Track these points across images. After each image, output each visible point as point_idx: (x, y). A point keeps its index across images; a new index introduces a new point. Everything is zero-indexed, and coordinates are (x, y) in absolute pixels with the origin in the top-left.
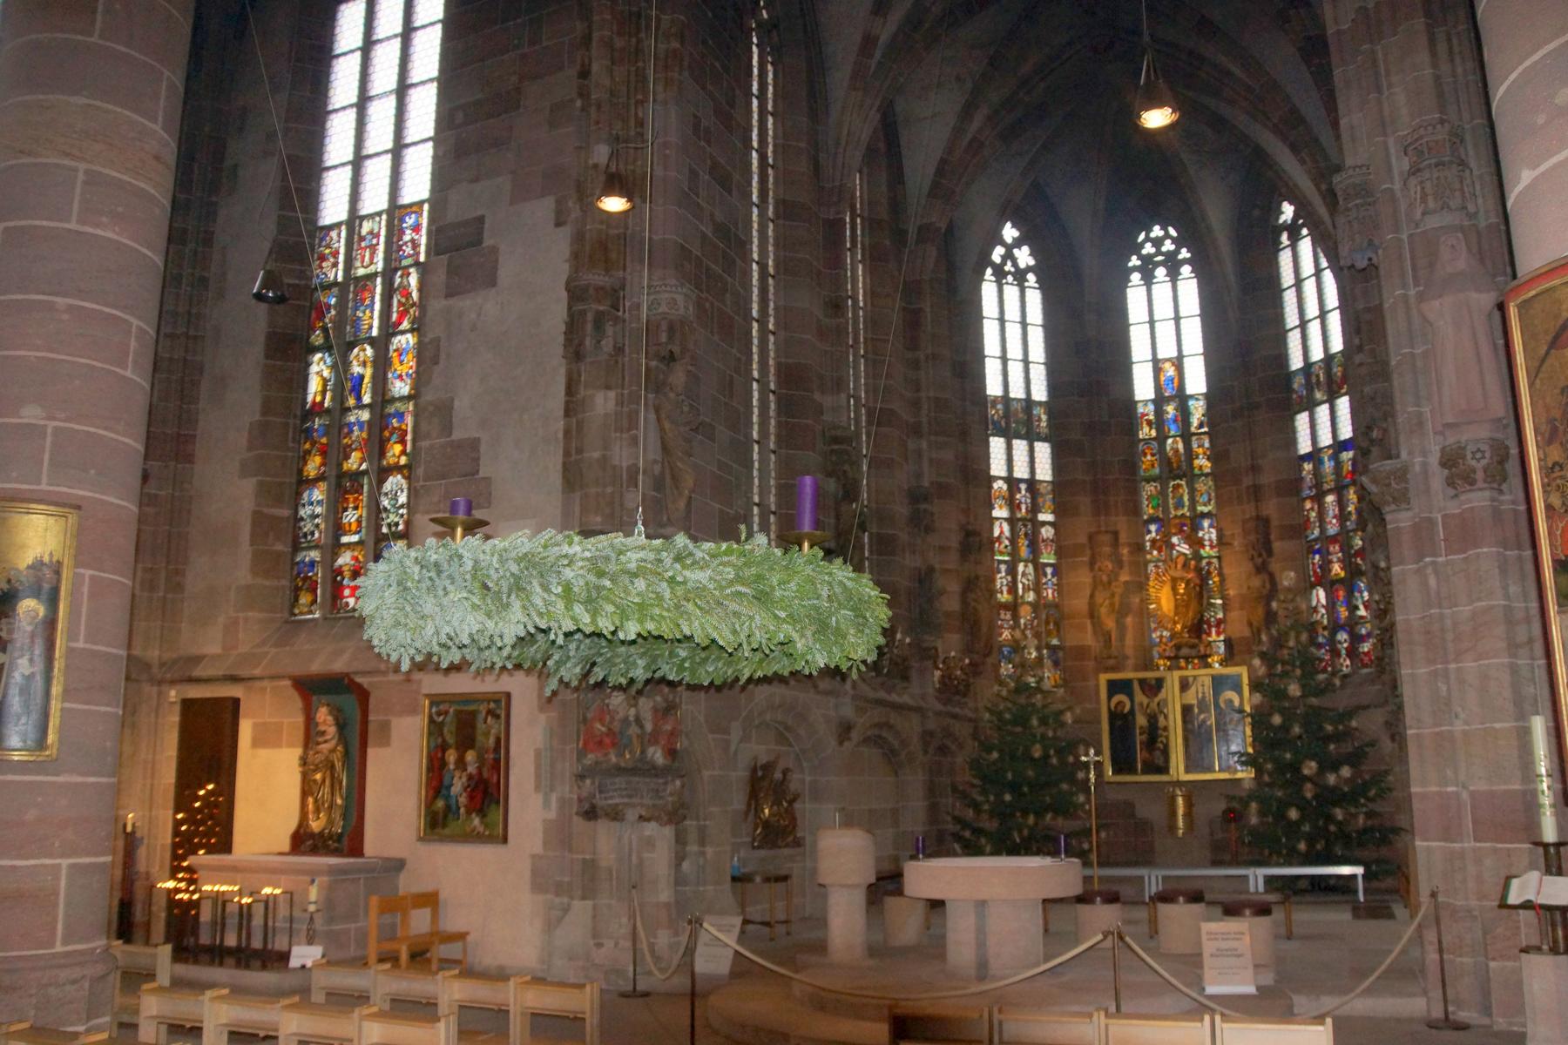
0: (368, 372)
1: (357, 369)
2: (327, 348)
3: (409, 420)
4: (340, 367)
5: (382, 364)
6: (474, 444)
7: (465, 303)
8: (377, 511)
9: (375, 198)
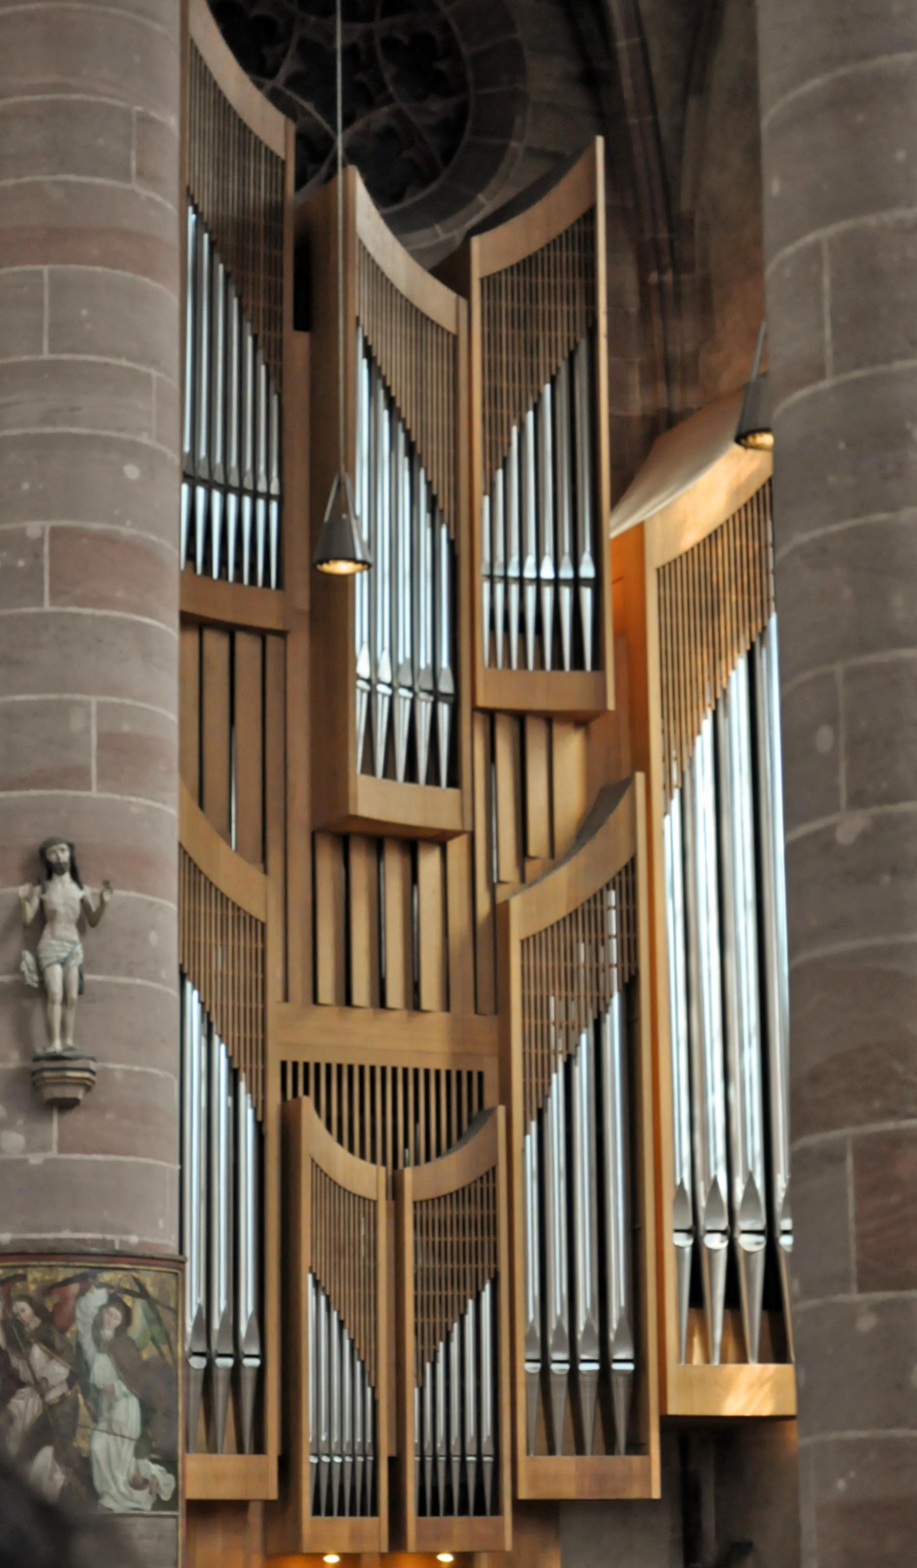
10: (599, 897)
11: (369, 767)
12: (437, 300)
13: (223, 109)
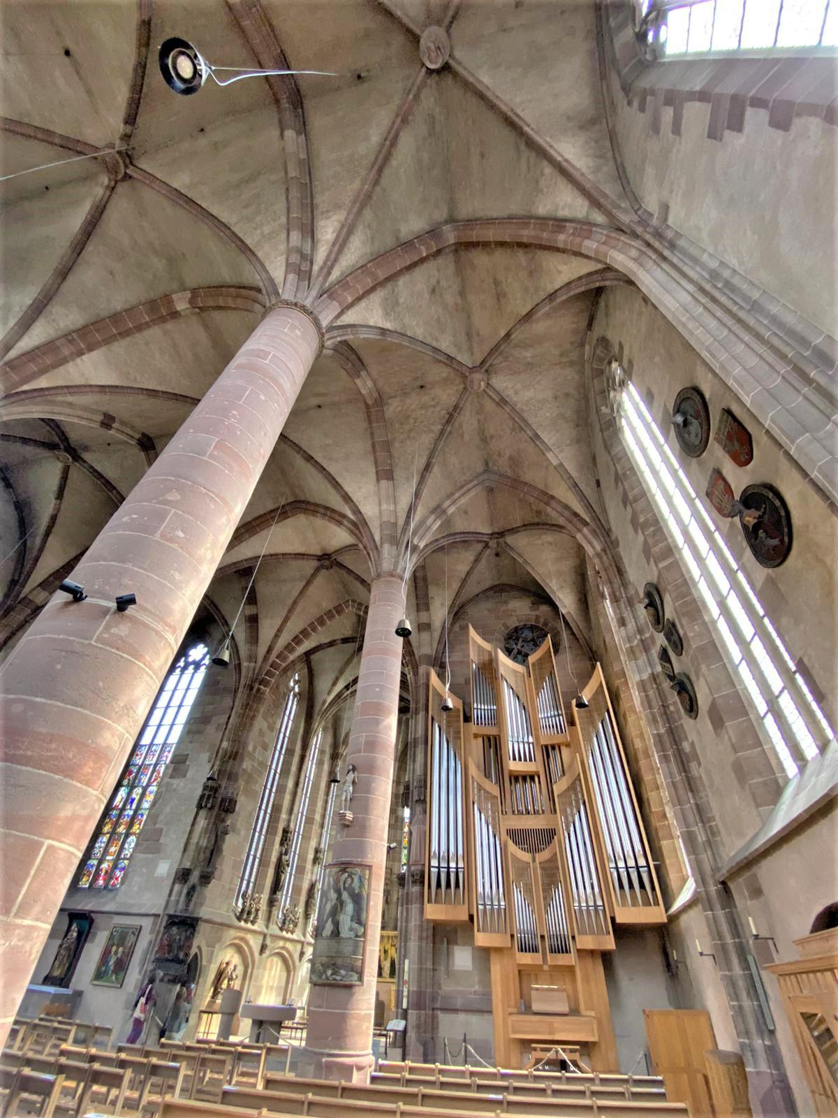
0: (137, 798)
1: (134, 796)
2: (127, 786)
3: (145, 817)
4: (129, 794)
5: (143, 795)
6: (161, 830)
7: (175, 782)
8: (122, 848)
9: (160, 740)
10: (574, 783)
11: (514, 759)
12: (520, 668)
13: (479, 646)
